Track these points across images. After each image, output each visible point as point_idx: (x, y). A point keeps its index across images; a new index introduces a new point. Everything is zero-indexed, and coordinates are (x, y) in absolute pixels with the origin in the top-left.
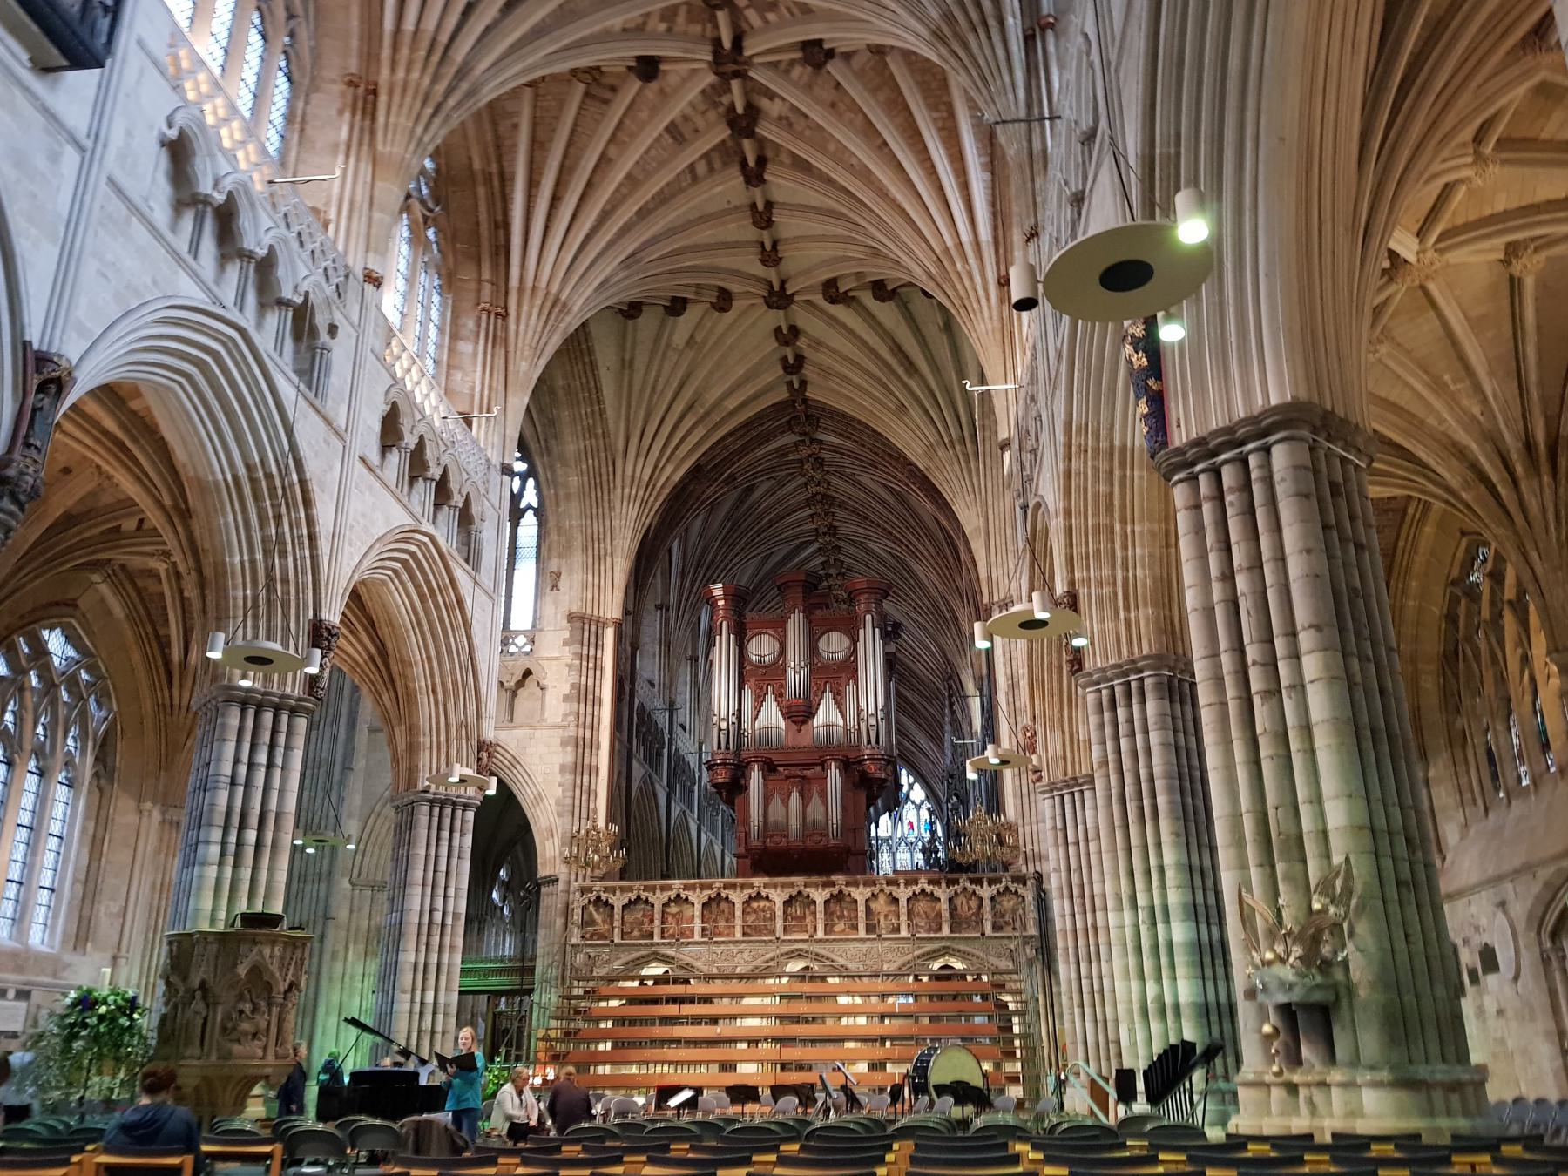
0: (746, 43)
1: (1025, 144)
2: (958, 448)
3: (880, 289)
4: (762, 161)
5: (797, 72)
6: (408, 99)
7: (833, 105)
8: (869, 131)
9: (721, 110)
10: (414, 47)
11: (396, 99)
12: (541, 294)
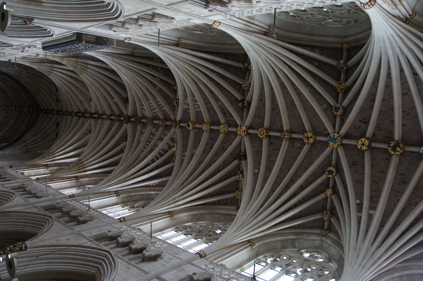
0: (94, 119)
1: (56, 177)
2: (25, 148)
3: (57, 134)
4: (79, 116)
5: (90, 128)
6: (75, 64)
7: (84, 134)
8: (79, 140)
9: (87, 111)
10: (85, 67)
11: (75, 62)
12: (51, 71)
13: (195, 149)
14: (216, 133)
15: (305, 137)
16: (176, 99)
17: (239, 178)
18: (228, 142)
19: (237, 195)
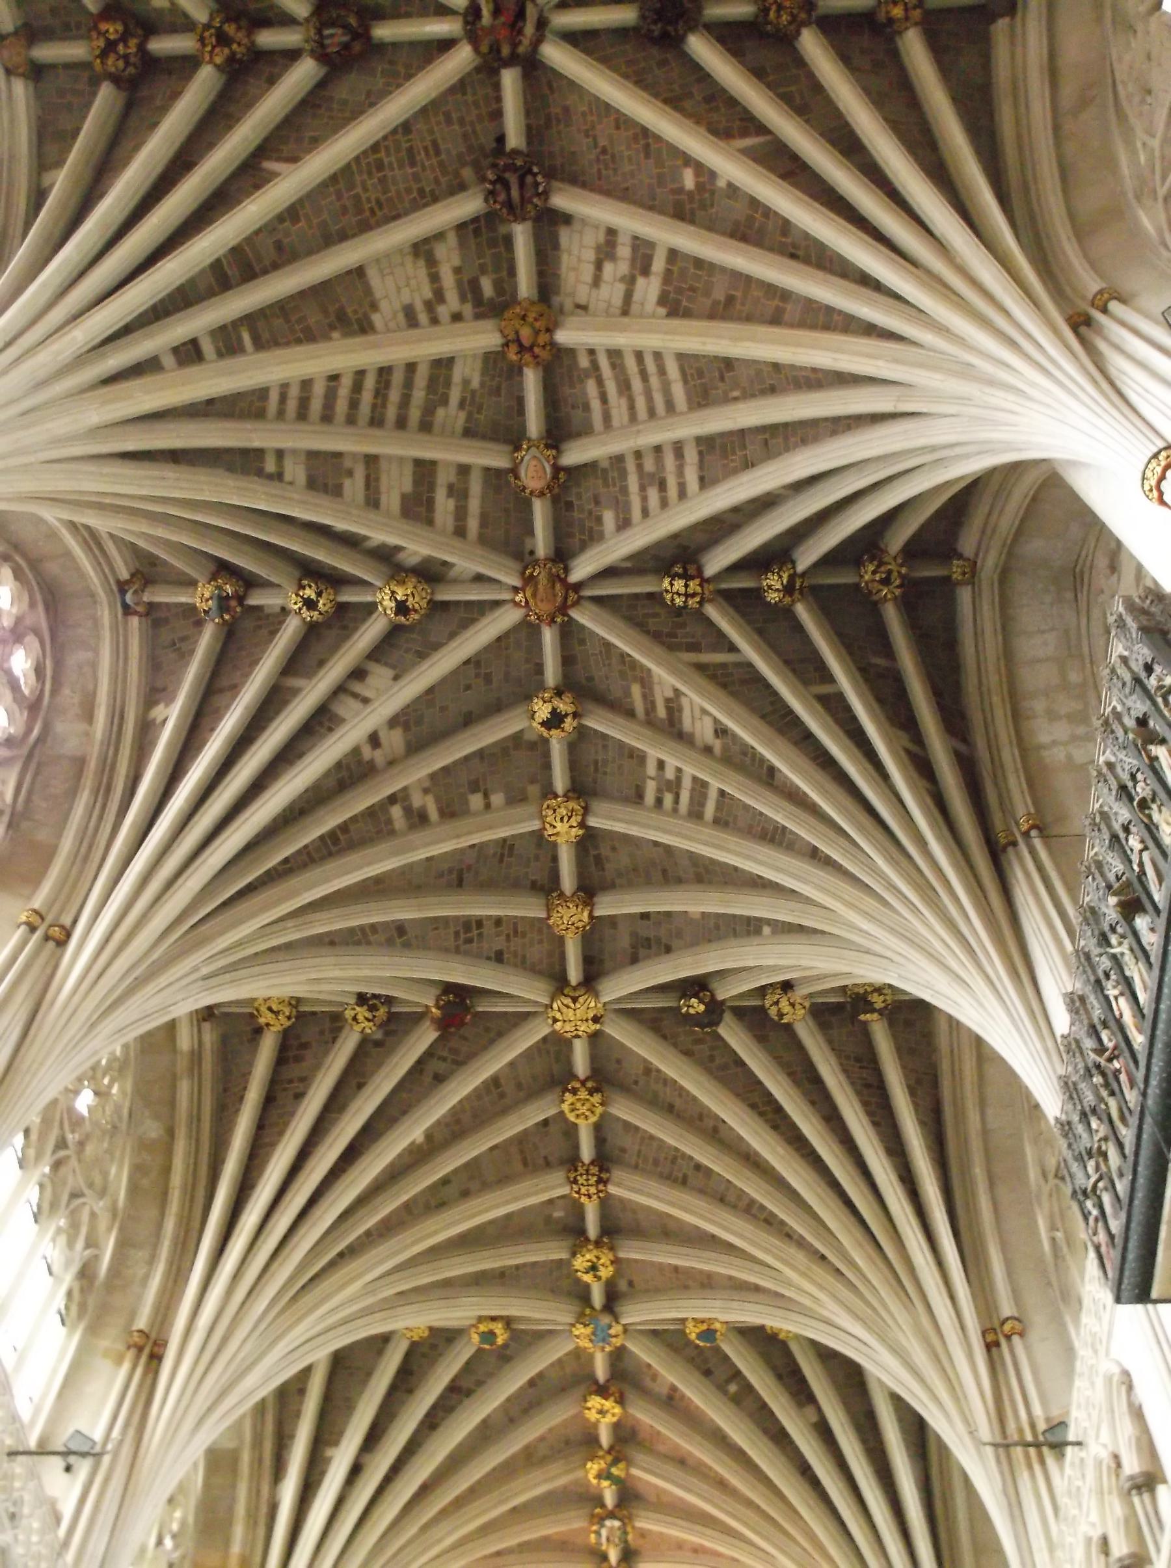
13: (427, 784)
14: (537, 858)
15: (595, 1260)
16: (701, 603)
17: (355, 1019)
18: (508, 936)
19: (270, 1009)
